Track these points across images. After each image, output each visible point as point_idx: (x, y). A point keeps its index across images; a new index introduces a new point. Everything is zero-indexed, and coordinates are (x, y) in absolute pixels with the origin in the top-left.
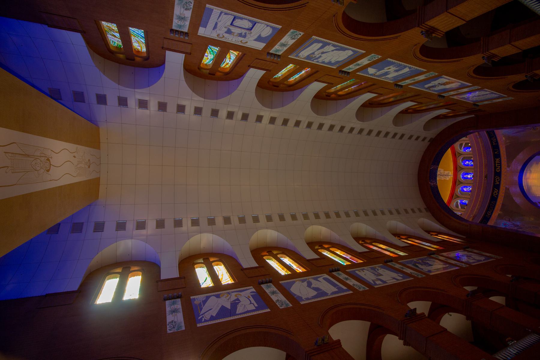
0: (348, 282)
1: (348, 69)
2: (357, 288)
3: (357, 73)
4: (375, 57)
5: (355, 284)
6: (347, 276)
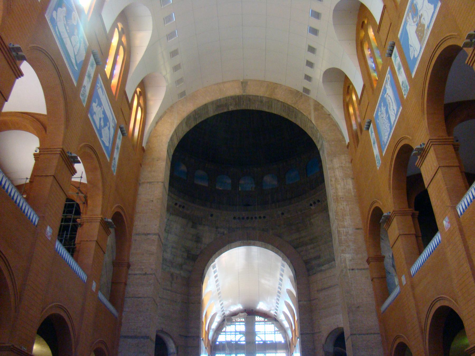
0: (86, 79)
1: (395, 55)
2: (82, 92)
3: (389, 67)
4: (405, 90)
5: (86, 88)
6: (92, 76)
